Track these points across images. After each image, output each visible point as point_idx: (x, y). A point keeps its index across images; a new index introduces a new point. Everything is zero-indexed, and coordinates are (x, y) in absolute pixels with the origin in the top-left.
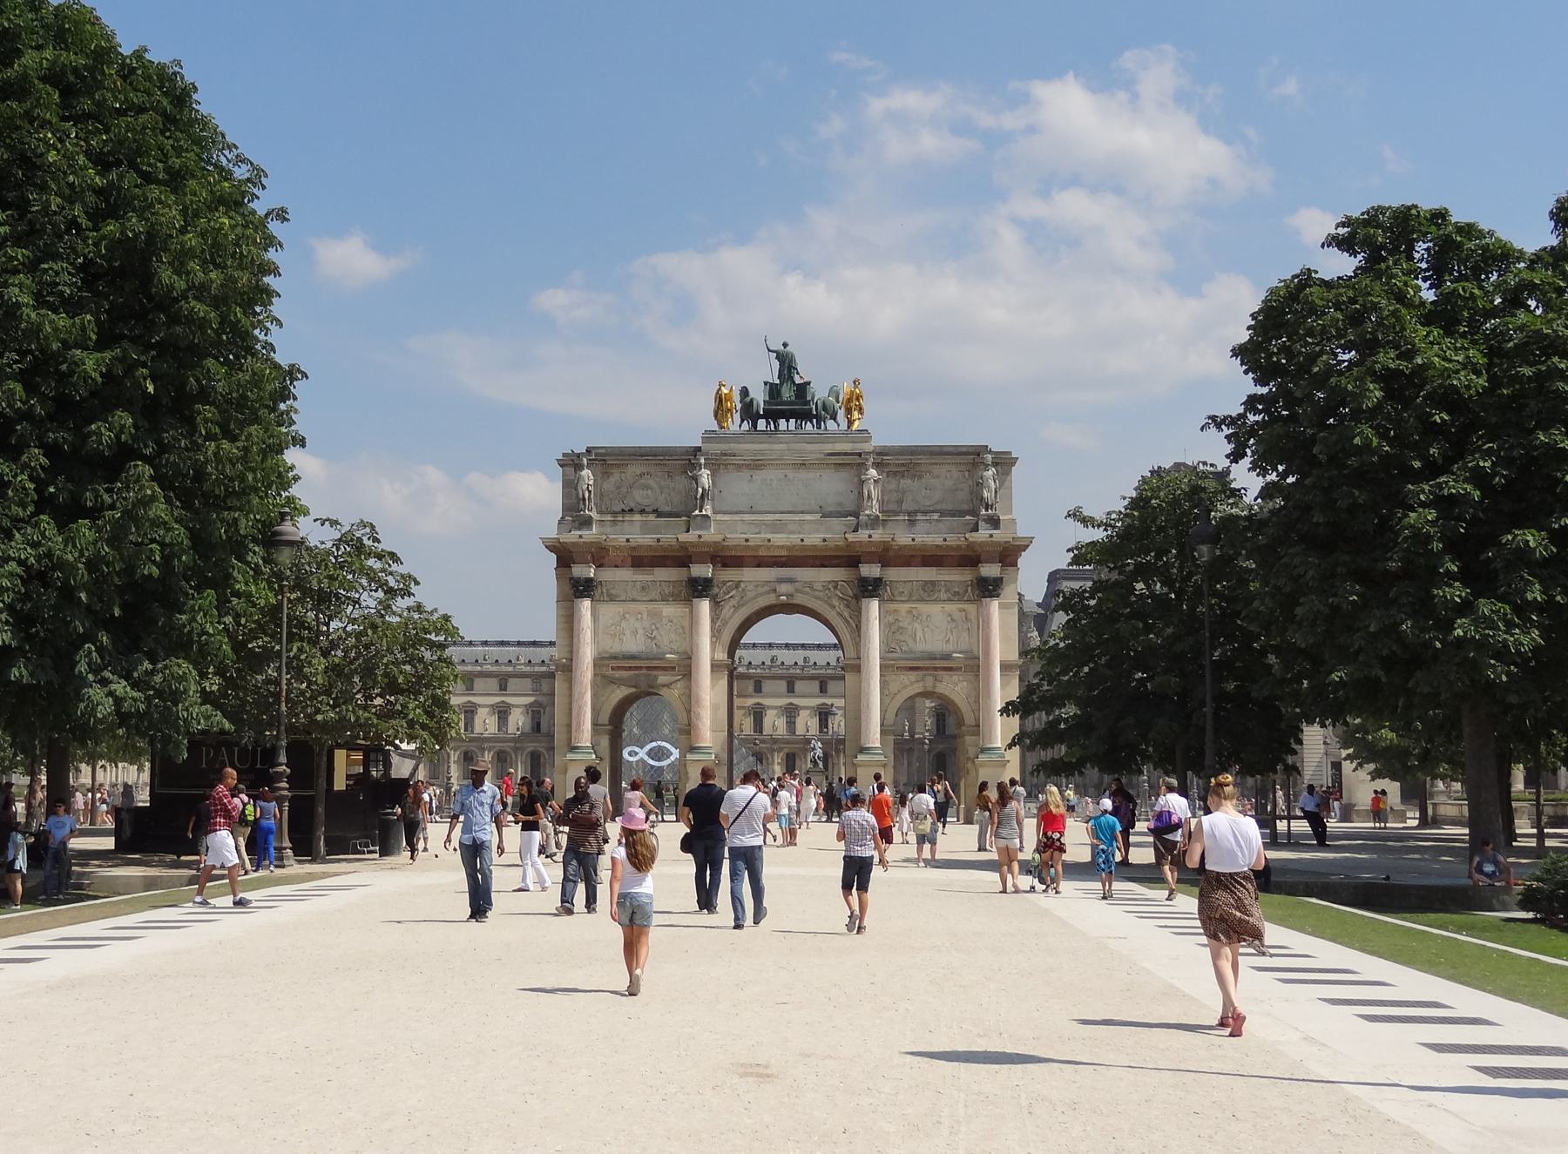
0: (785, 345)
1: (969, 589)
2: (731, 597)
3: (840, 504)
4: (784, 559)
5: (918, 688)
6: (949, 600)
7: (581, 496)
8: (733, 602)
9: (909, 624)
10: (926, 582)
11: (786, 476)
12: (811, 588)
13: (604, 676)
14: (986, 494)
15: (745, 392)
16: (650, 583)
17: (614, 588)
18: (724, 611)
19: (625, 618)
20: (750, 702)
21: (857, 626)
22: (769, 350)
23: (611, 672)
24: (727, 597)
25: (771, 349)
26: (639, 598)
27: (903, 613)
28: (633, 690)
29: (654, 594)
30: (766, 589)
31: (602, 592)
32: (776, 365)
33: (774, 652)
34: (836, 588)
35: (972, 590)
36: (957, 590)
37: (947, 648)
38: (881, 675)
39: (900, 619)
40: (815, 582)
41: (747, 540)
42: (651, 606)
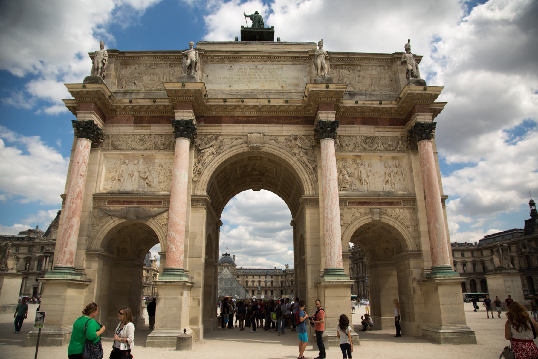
1: (400, 142)
2: (211, 146)
3: (297, 85)
4: (254, 119)
5: (366, 220)
6: (386, 150)
7: (96, 67)
8: (212, 150)
9: (356, 169)
10: (367, 137)
11: (256, 66)
12: (276, 140)
13: (101, 209)
14: (410, 67)
16: (146, 137)
17: (118, 140)
18: (204, 158)
19: (125, 163)
20: (245, 280)
21: (314, 169)
22: (246, 16)
23: (107, 205)
24: (208, 146)
25: (247, 14)
26: (137, 147)
27: (350, 161)
28: (123, 221)
29: (149, 144)
30: (240, 141)
31: (108, 143)
33: (250, 270)
34: (295, 139)
35: (402, 143)
36: (390, 143)
37: (388, 188)
39: (348, 165)
40: (279, 135)
41: (225, 101)
42: (146, 153)
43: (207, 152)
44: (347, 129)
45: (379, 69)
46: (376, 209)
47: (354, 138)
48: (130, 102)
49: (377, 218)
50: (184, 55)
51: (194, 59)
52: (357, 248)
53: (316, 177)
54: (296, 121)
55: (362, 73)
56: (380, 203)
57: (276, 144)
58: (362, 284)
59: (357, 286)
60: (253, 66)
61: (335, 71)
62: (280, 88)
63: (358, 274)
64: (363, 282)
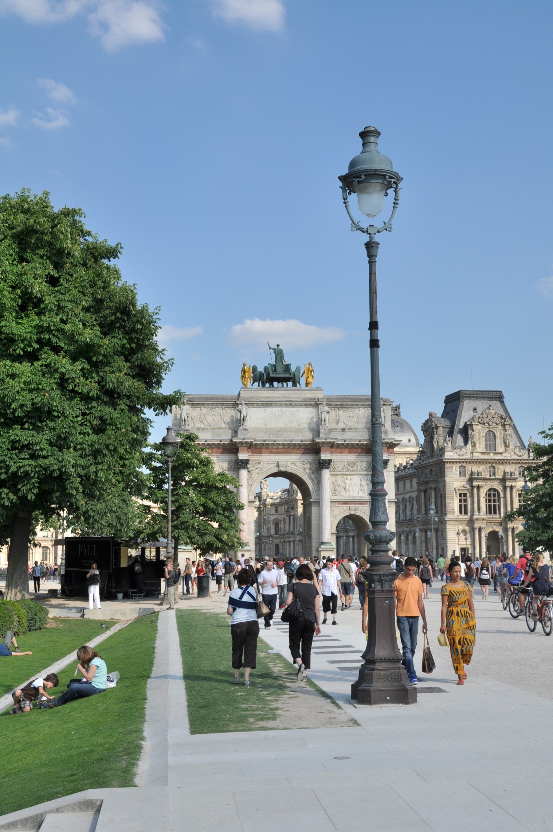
0: (278, 346)
5: (347, 513)
8: (257, 471)
10: (351, 462)
15: (255, 369)
22: (270, 348)
25: (271, 347)
32: (274, 355)
38: (331, 507)
41: (264, 441)
43: (255, 472)
44: (339, 457)
45: (363, 409)
46: (353, 506)
47: (343, 463)
48: (206, 441)
49: (353, 512)
50: (238, 410)
51: (245, 415)
52: (427, 458)
53: (319, 488)
54: (307, 451)
55: (352, 414)
56: (356, 504)
57: (295, 467)
58: (434, 535)
59: (423, 538)
60: (279, 409)
61: (333, 412)
62: (298, 426)
63: (426, 513)
64: (437, 530)
